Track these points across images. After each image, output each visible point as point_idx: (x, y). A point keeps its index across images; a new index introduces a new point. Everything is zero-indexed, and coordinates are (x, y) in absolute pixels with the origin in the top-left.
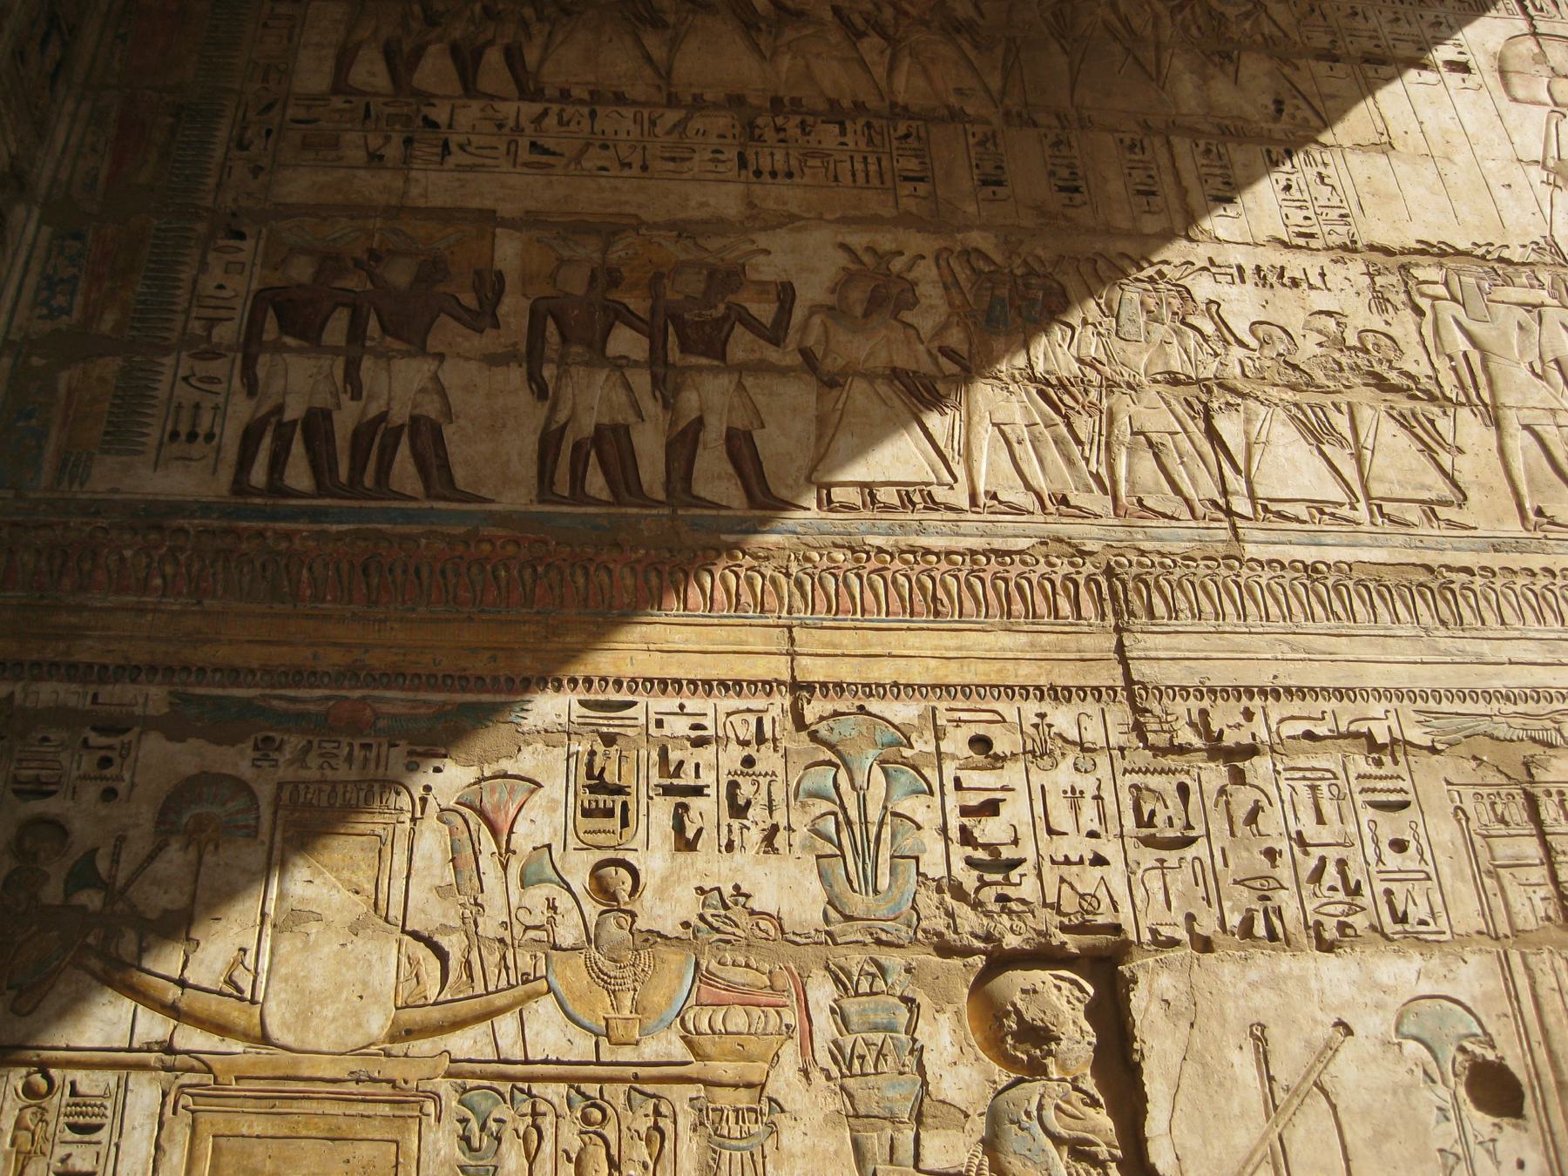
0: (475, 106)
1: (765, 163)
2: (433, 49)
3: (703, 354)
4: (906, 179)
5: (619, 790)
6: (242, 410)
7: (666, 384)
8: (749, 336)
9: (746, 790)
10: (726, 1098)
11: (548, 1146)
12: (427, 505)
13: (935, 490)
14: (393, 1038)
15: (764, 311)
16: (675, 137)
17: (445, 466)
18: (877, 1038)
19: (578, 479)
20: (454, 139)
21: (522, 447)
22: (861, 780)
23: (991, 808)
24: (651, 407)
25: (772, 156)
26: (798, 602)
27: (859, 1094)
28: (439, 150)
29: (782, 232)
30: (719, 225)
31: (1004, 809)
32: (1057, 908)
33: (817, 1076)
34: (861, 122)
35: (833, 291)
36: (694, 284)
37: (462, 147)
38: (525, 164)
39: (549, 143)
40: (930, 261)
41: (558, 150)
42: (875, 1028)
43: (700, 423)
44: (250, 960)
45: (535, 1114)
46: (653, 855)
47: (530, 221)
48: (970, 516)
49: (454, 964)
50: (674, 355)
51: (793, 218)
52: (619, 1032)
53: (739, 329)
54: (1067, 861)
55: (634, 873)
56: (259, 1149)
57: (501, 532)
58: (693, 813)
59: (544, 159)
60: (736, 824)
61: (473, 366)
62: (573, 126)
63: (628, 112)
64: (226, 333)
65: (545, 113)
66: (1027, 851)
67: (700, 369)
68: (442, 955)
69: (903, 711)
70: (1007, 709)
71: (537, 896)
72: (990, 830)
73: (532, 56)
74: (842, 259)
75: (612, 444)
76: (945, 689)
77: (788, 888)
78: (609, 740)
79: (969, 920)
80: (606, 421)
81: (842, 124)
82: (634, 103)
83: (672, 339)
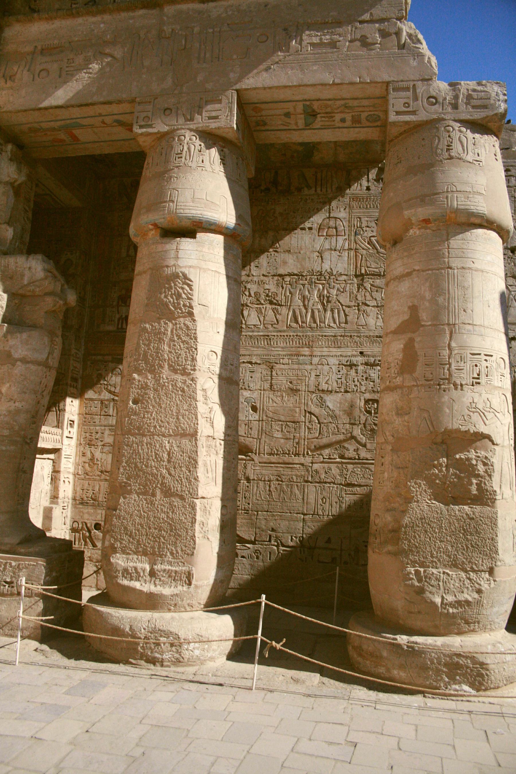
6: (118, 316)
64: (115, 303)
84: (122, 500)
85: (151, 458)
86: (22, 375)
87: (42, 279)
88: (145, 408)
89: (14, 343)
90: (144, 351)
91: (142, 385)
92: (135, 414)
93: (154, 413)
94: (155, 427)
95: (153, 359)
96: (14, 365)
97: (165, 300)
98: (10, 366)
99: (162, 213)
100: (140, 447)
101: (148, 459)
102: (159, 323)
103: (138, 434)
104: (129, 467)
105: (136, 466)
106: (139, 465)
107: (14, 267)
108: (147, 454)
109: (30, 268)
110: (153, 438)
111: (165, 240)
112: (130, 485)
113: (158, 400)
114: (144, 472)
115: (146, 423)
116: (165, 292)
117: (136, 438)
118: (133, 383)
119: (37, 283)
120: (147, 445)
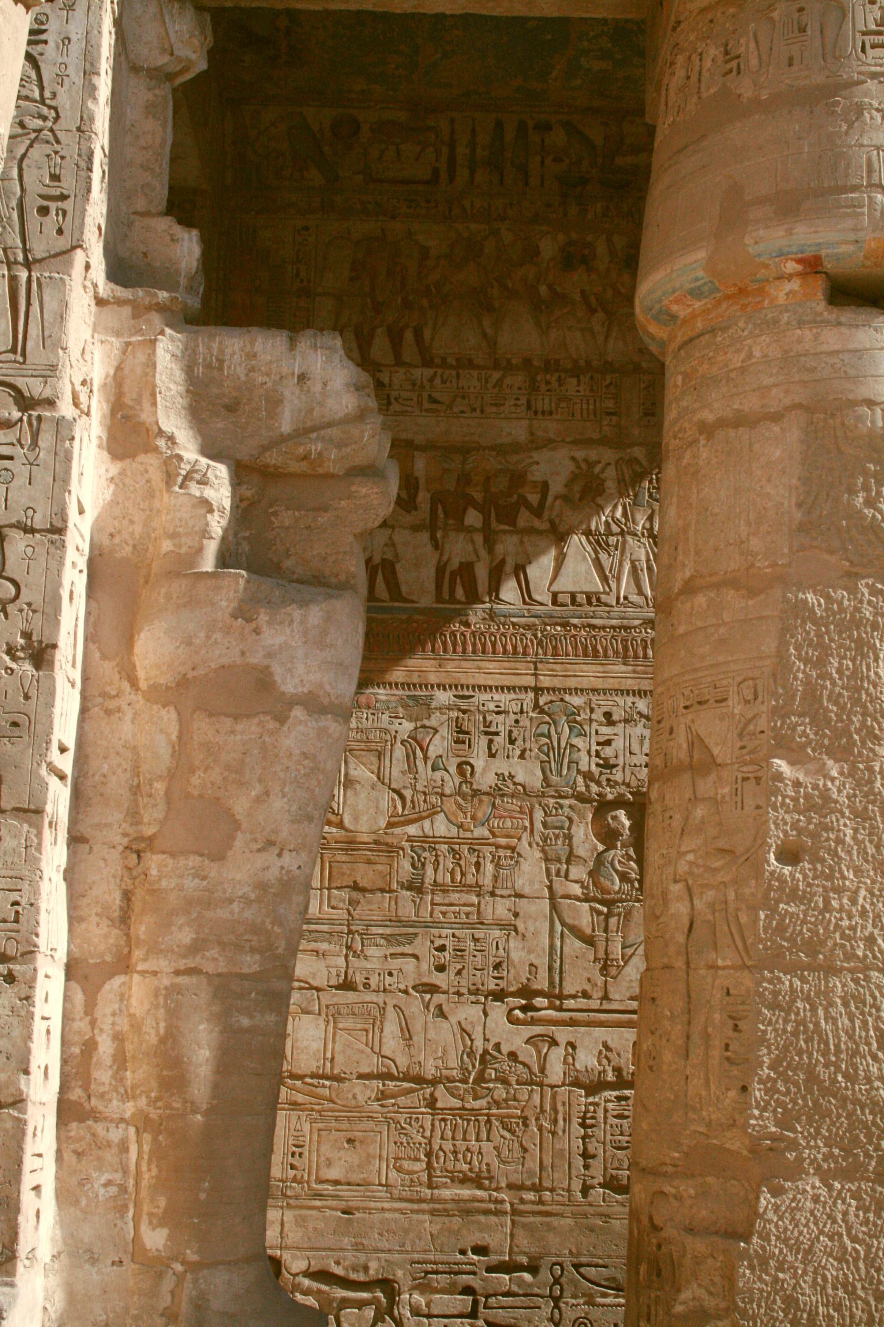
0: (402, 370)
1: (540, 406)
2: (379, 331)
3: (506, 524)
4: (608, 414)
5: (467, 733)
7: (490, 542)
8: (527, 513)
9: (515, 734)
10: (502, 853)
11: (441, 867)
12: (391, 604)
13: (602, 596)
14: (387, 828)
15: (534, 498)
16: (496, 390)
17: (397, 584)
18: (557, 831)
19: (452, 591)
20: (394, 394)
21: (428, 573)
22: (559, 730)
23: (608, 743)
24: (483, 553)
25: (544, 403)
26: (540, 651)
27: (550, 852)
28: (385, 402)
29: (545, 450)
30: (517, 447)
31: (614, 744)
32: (628, 785)
33: (535, 845)
34: (588, 376)
35: (566, 486)
36: (501, 484)
37: (396, 399)
38: (426, 410)
39: (437, 395)
40: (613, 467)
41: (439, 399)
42: (556, 828)
43: (503, 562)
44: (336, 799)
45: (437, 856)
46: (479, 761)
47: (428, 447)
48: (616, 609)
49: (409, 803)
50: (494, 525)
51: (551, 441)
52: (466, 827)
53: (523, 510)
54: (635, 766)
55: (472, 767)
56: (344, 866)
57: (421, 618)
58: (495, 743)
59: (435, 406)
60: (511, 747)
61: (406, 532)
62: (448, 385)
63: (475, 373)
65: (435, 373)
66: (621, 761)
67: (505, 532)
68: (402, 797)
69: (577, 701)
70: (620, 700)
71: (438, 775)
72: (608, 752)
73: (427, 334)
74: (571, 466)
75: (466, 571)
76: (595, 690)
77: (528, 774)
78: (464, 712)
79: (594, 788)
80: (463, 560)
81: (578, 377)
82: (478, 367)
83: (493, 515)
84: (765, 1200)
85: (863, 1048)
86: (305, 756)
87: (347, 420)
88: (830, 877)
89: (279, 640)
90: (807, 682)
91: (807, 796)
92: (794, 896)
93: (863, 893)
94: (871, 941)
95: (842, 708)
96: (281, 719)
97: (869, 512)
98: (272, 725)
99: (849, 223)
100: (821, 1012)
101: (856, 1053)
102: (853, 591)
103: (811, 968)
104: (786, 1081)
105: (812, 1078)
106: (823, 1073)
107: (241, 371)
108: (851, 1037)
109: (302, 378)
110: (867, 979)
111: (847, 315)
112: (793, 1145)
113: (871, 850)
114: (845, 1099)
115: (837, 926)
116: (866, 488)
117: (803, 980)
118: (776, 792)
119: (334, 432)
120: (846, 1004)
